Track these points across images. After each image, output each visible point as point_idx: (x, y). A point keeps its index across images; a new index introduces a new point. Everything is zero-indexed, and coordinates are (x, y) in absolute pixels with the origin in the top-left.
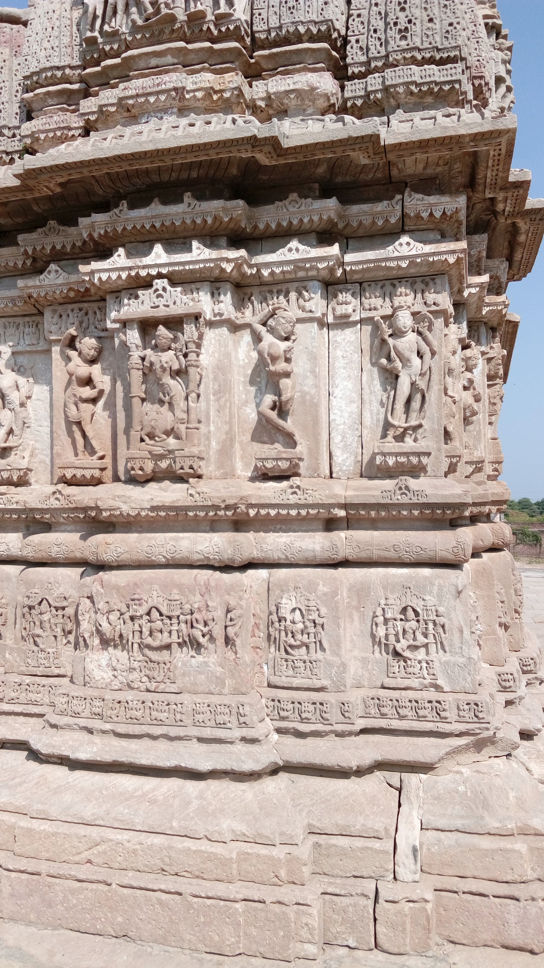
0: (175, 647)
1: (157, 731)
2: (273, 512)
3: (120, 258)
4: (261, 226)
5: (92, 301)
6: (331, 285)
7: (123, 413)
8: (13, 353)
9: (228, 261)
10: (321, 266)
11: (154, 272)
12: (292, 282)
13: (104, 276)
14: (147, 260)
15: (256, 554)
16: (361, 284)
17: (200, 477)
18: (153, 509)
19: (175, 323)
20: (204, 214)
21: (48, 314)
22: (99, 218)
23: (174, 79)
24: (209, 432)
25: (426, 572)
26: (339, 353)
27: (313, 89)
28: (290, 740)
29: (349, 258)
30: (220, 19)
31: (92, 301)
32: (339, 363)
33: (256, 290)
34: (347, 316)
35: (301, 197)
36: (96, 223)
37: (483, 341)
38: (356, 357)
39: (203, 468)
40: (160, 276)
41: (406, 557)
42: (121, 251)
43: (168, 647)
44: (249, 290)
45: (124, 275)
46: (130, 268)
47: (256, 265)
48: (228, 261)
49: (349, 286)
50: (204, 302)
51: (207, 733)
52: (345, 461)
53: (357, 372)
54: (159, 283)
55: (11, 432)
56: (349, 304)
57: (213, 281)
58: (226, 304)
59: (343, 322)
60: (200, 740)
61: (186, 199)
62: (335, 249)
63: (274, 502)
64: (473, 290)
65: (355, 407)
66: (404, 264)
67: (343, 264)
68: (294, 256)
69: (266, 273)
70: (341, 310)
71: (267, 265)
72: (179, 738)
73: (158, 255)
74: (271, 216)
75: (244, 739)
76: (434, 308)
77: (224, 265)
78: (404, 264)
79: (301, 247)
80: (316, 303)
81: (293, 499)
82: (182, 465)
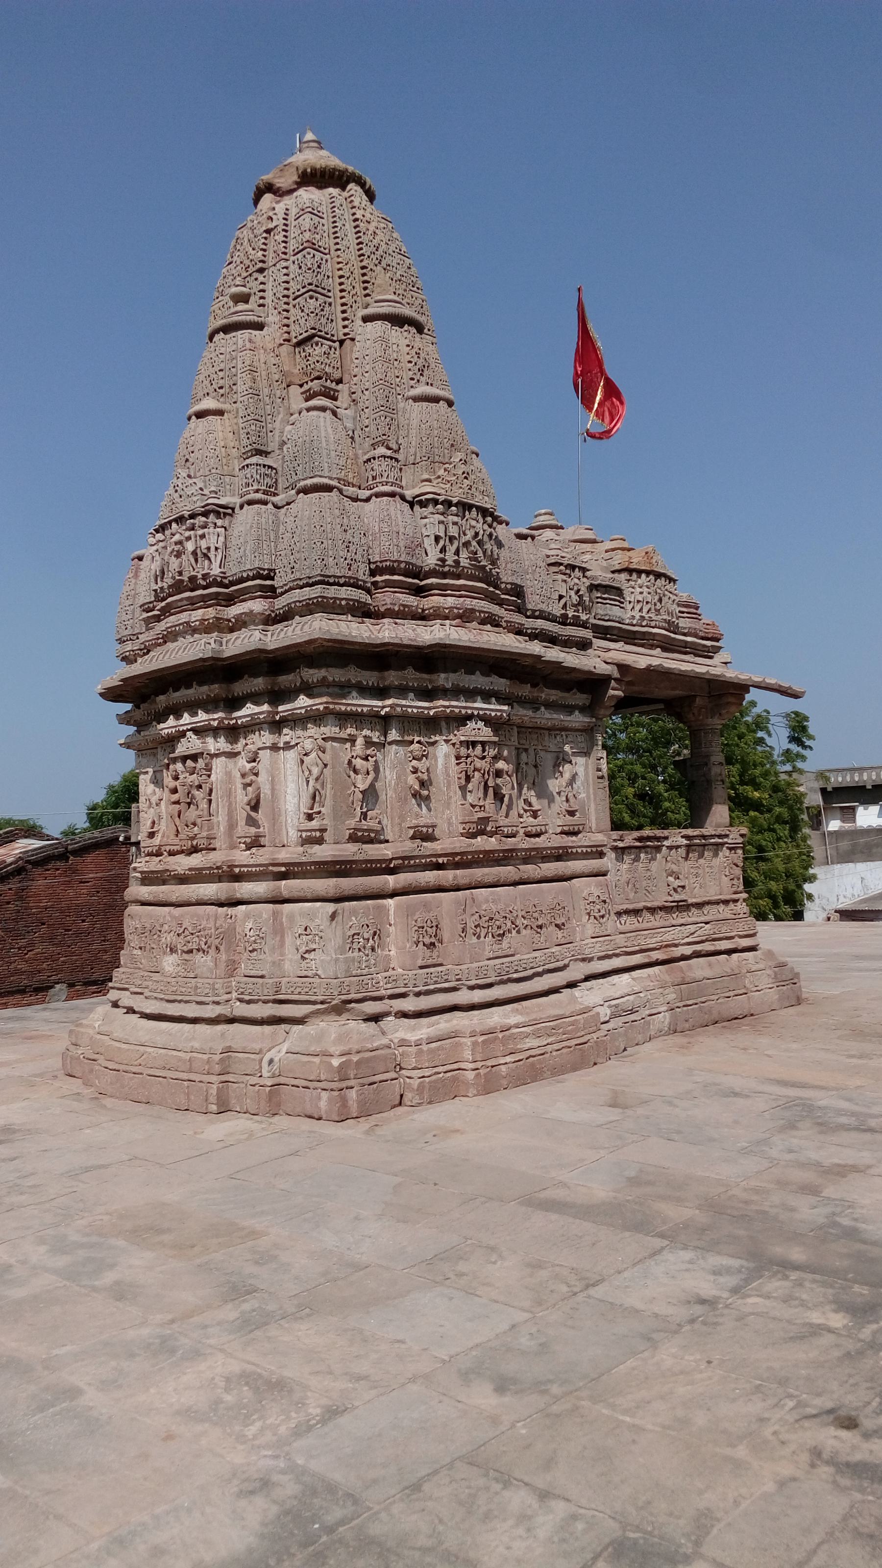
0: (194, 951)
1: (179, 998)
2: (246, 870)
3: (171, 721)
4: (236, 694)
6: (277, 726)
8: (154, 772)
9: (214, 720)
10: (261, 717)
11: (185, 728)
13: (166, 731)
14: (182, 722)
16: (294, 721)
17: (215, 849)
18: (190, 869)
19: (194, 757)
20: (203, 693)
21: (159, 749)
22: (161, 698)
23: (184, 617)
24: (219, 822)
25: (318, 904)
26: (288, 765)
27: (252, 611)
28: (244, 1005)
29: (281, 708)
30: (205, 576)
32: (289, 772)
33: (242, 730)
34: (289, 743)
35: (250, 677)
36: (162, 700)
37: (444, 731)
38: (296, 767)
39: (217, 844)
40: (189, 730)
41: (309, 896)
42: (171, 717)
43: (191, 951)
44: (239, 731)
45: (174, 730)
46: (176, 727)
47: (235, 718)
48: (214, 720)
49: (289, 723)
50: (213, 744)
53: (296, 778)
54: (189, 734)
55: (154, 823)
56: (288, 735)
57: (215, 732)
58: (220, 744)
59: (288, 747)
60: (198, 1003)
61: (194, 686)
62: (266, 707)
63: (245, 863)
64: (387, 709)
65: (296, 800)
66: (303, 711)
67: (277, 713)
68: (249, 712)
69: (239, 722)
70: (287, 739)
71: (240, 717)
72: (187, 1002)
73: (186, 718)
74: (240, 688)
75: (214, 1002)
76: (324, 736)
77: (212, 723)
78: (303, 711)
79: (252, 706)
80: (266, 738)
81: (252, 862)
82: (201, 842)
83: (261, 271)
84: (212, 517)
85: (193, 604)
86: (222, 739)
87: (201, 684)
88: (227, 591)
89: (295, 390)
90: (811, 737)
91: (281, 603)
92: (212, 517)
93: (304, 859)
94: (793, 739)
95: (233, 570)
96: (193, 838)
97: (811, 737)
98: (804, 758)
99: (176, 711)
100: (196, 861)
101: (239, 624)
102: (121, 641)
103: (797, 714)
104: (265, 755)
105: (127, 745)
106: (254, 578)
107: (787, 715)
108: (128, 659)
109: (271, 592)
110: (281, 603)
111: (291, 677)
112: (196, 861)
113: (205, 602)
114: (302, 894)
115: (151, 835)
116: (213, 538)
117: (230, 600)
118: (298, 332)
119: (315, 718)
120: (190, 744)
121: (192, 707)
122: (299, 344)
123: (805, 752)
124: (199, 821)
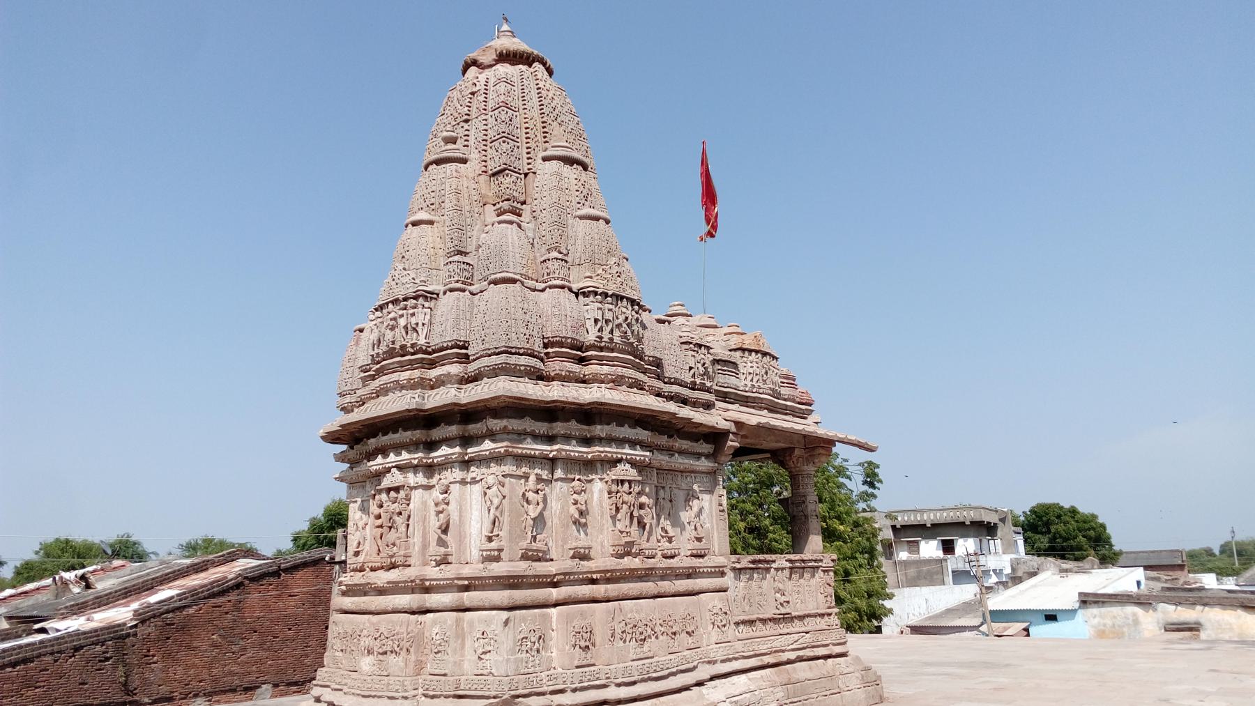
3: (379, 459)
5: (379, 475)
6: (466, 464)
7: (212, 571)
12: (445, 465)
15: (428, 605)
19: (397, 489)
22: (372, 441)
25: (494, 612)
29: (469, 450)
30: (413, 345)
31: (379, 475)
39: (411, 561)
41: (487, 605)
43: (385, 653)
50: (412, 479)
51: (390, 694)
52: (476, 554)
54: (394, 470)
56: (474, 472)
58: (420, 479)
59: (474, 481)
60: (389, 698)
62: (458, 449)
68: (443, 453)
70: (474, 475)
72: (380, 697)
73: (392, 457)
74: (437, 433)
80: (457, 474)
81: (440, 576)
82: (399, 560)
83: (466, 121)
84: (421, 300)
85: (402, 367)
86: (420, 475)
87: (405, 430)
88: (430, 357)
89: (489, 208)
90: (880, 481)
91: (472, 367)
92: (421, 300)
93: (484, 574)
94: (865, 483)
95: (436, 341)
96: (392, 557)
97: (880, 481)
98: (875, 496)
99: (383, 451)
100: (394, 575)
101: (439, 383)
102: (341, 395)
103: (870, 463)
104: (455, 488)
105: (341, 479)
106: (452, 348)
107: (861, 464)
108: (346, 410)
109: (466, 359)
110: (472, 367)
111: (479, 425)
112: (394, 575)
113: (412, 365)
114: (481, 604)
115: (357, 554)
116: (421, 316)
117: (432, 364)
118: (493, 166)
119: (498, 459)
120: (394, 478)
121: (398, 448)
122: (494, 175)
123: (876, 492)
124: (398, 542)
